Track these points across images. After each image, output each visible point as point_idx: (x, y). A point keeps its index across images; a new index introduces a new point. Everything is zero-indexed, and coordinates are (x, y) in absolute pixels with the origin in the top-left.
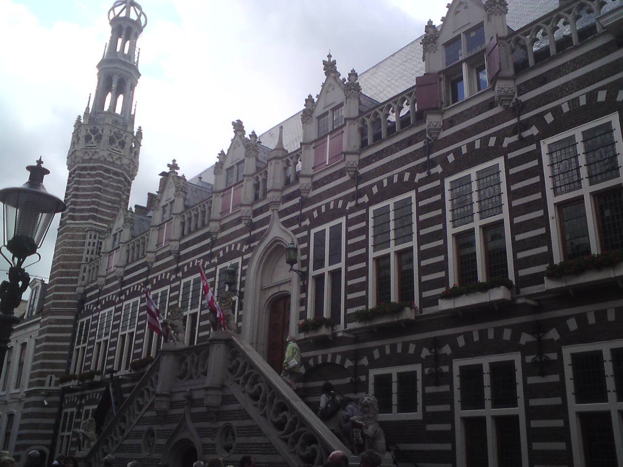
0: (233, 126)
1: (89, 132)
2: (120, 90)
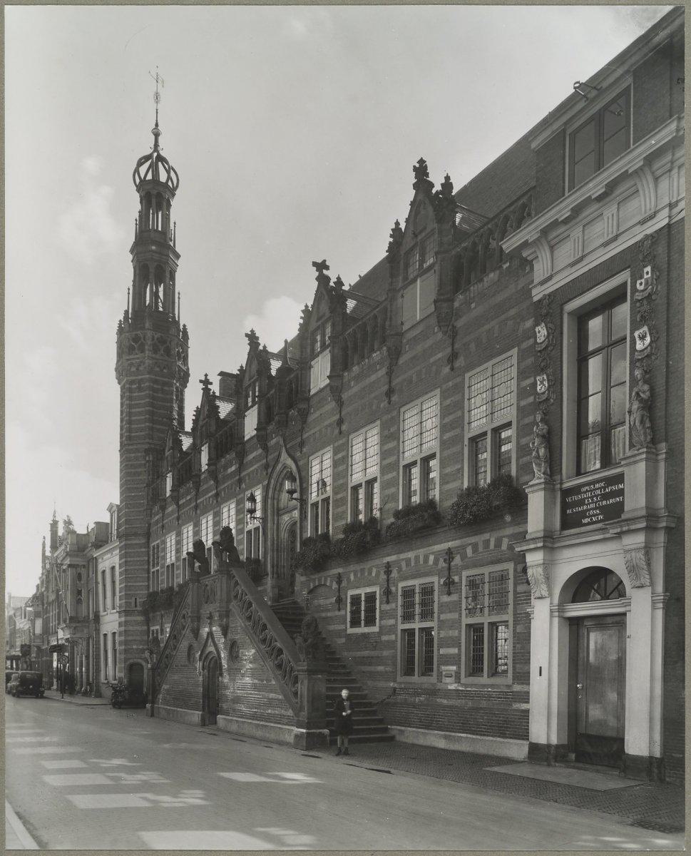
0: (315, 268)
2: (159, 279)
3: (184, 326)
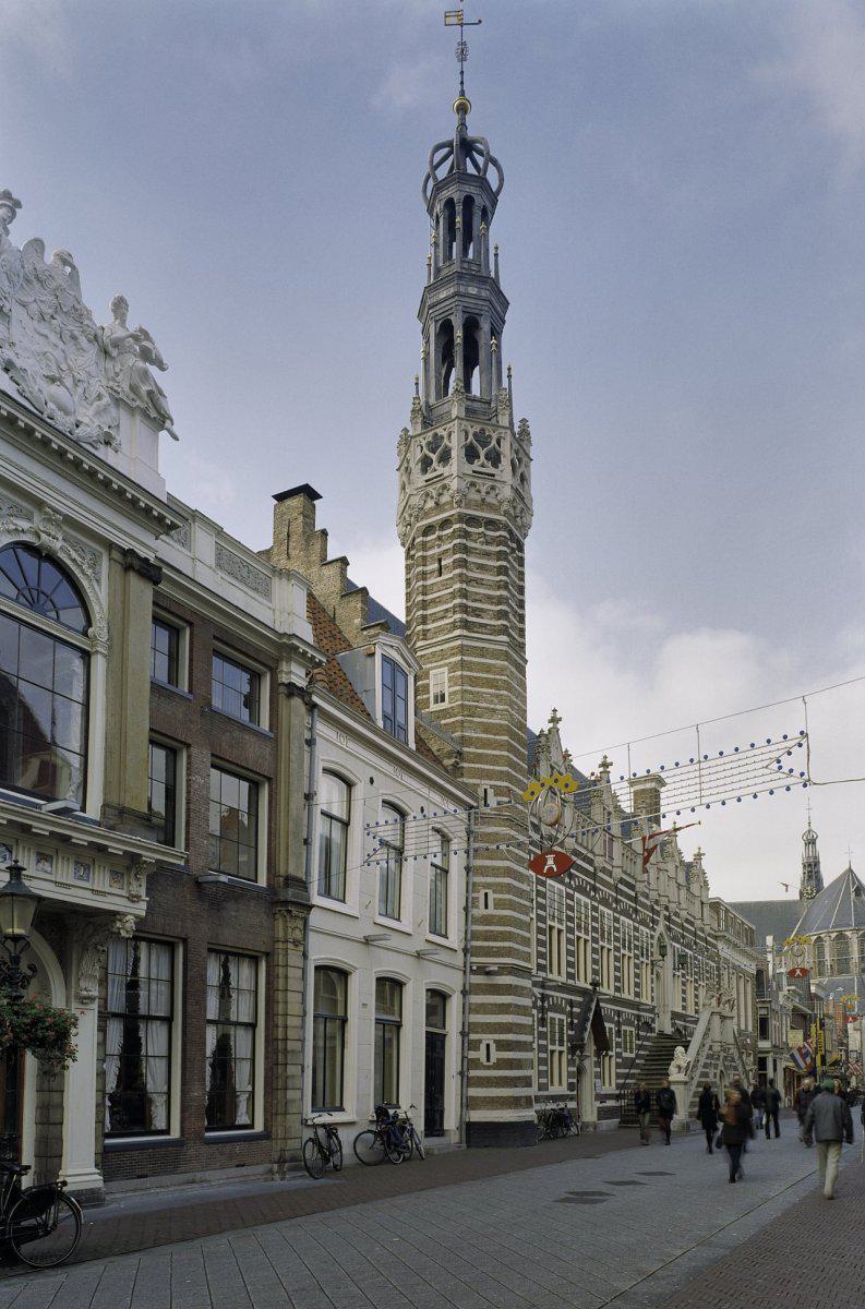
3: (524, 421)
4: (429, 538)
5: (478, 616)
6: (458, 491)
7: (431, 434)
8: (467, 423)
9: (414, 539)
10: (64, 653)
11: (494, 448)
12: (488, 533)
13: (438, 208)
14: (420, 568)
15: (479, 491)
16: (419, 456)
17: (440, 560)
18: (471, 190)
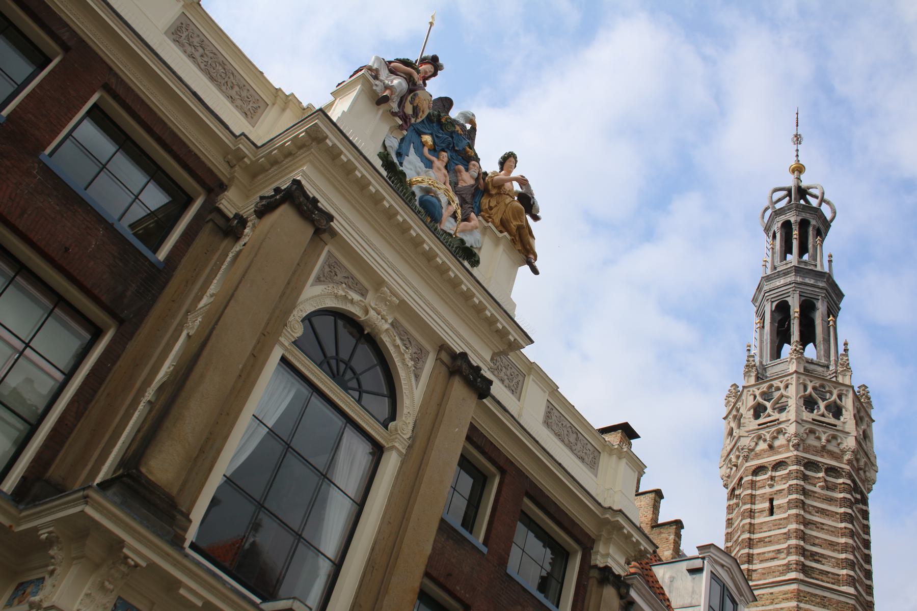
1: (759, 399)
4: (758, 478)
5: (817, 561)
6: (796, 435)
7: (766, 385)
8: (806, 378)
9: (741, 479)
10: (351, 439)
11: (835, 402)
12: (829, 479)
13: (777, 226)
14: (748, 506)
15: (819, 438)
16: (751, 402)
17: (771, 500)
18: (807, 216)
